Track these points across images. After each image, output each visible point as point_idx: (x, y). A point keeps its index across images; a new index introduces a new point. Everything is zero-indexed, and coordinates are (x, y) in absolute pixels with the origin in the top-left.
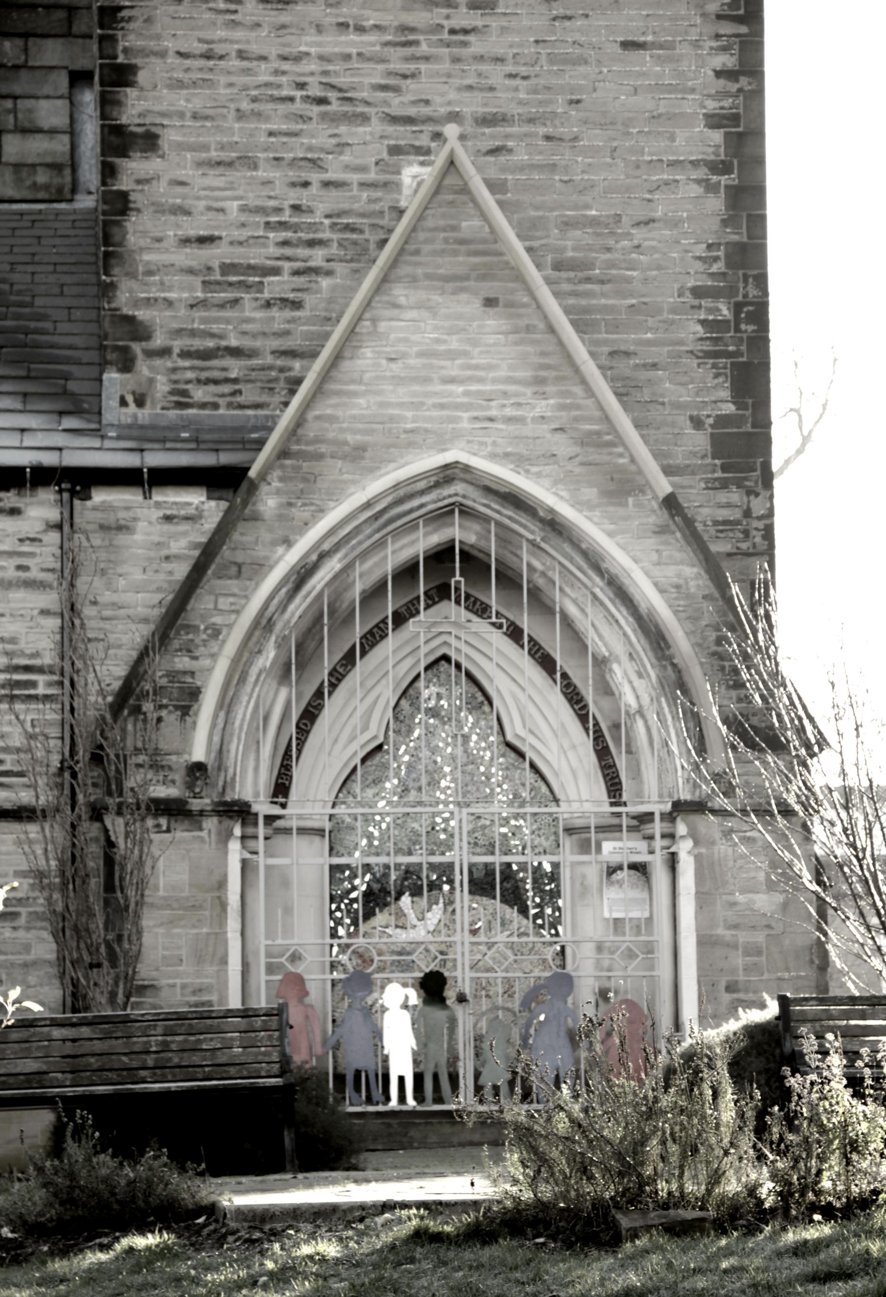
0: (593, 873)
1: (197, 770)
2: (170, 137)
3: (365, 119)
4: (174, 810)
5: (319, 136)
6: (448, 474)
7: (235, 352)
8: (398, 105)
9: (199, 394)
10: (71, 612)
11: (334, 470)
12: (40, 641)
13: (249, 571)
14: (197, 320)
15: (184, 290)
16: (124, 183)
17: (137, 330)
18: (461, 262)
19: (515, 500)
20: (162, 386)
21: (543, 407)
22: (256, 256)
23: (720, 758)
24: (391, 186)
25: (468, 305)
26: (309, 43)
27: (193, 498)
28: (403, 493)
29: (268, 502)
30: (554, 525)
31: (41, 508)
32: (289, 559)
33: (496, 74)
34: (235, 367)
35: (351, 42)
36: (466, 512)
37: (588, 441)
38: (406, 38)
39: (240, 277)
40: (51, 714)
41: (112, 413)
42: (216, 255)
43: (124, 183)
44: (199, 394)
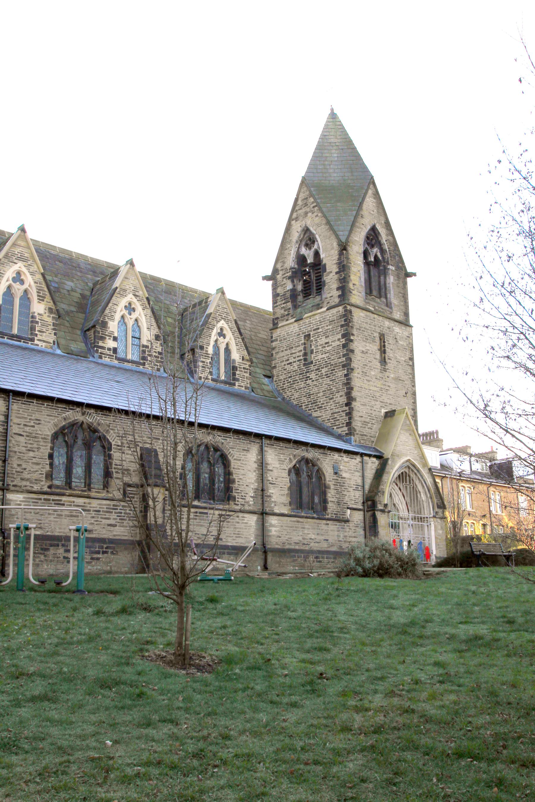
0: (407, 526)
1: (386, 505)
2: (358, 399)
3: (377, 401)
4: (383, 511)
5: (373, 403)
6: (409, 461)
7: (365, 435)
8: (381, 399)
9: (362, 441)
10: (363, 476)
11: (396, 458)
12: (360, 482)
13: (389, 473)
14: (361, 429)
15: (359, 424)
16: (353, 406)
17: (355, 430)
18: (407, 428)
19: (414, 466)
20: (358, 440)
21: (416, 452)
22: (367, 420)
23: (437, 509)
24: (381, 412)
25: (408, 434)
26: (371, 388)
27: (374, 460)
28: (403, 463)
29: (390, 462)
30: (418, 471)
31: (358, 458)
32: (394, 471)
33: (391, 397)
34: (365, 438)
35: (375, 389)
36: (409, 468)
37: (420, 458)
38: (381, 389)
39: (365, 423)
40: (361, 493)
41: (353, 443)
42: (363, 419)
43: (353, 406)
44: (362, 441)
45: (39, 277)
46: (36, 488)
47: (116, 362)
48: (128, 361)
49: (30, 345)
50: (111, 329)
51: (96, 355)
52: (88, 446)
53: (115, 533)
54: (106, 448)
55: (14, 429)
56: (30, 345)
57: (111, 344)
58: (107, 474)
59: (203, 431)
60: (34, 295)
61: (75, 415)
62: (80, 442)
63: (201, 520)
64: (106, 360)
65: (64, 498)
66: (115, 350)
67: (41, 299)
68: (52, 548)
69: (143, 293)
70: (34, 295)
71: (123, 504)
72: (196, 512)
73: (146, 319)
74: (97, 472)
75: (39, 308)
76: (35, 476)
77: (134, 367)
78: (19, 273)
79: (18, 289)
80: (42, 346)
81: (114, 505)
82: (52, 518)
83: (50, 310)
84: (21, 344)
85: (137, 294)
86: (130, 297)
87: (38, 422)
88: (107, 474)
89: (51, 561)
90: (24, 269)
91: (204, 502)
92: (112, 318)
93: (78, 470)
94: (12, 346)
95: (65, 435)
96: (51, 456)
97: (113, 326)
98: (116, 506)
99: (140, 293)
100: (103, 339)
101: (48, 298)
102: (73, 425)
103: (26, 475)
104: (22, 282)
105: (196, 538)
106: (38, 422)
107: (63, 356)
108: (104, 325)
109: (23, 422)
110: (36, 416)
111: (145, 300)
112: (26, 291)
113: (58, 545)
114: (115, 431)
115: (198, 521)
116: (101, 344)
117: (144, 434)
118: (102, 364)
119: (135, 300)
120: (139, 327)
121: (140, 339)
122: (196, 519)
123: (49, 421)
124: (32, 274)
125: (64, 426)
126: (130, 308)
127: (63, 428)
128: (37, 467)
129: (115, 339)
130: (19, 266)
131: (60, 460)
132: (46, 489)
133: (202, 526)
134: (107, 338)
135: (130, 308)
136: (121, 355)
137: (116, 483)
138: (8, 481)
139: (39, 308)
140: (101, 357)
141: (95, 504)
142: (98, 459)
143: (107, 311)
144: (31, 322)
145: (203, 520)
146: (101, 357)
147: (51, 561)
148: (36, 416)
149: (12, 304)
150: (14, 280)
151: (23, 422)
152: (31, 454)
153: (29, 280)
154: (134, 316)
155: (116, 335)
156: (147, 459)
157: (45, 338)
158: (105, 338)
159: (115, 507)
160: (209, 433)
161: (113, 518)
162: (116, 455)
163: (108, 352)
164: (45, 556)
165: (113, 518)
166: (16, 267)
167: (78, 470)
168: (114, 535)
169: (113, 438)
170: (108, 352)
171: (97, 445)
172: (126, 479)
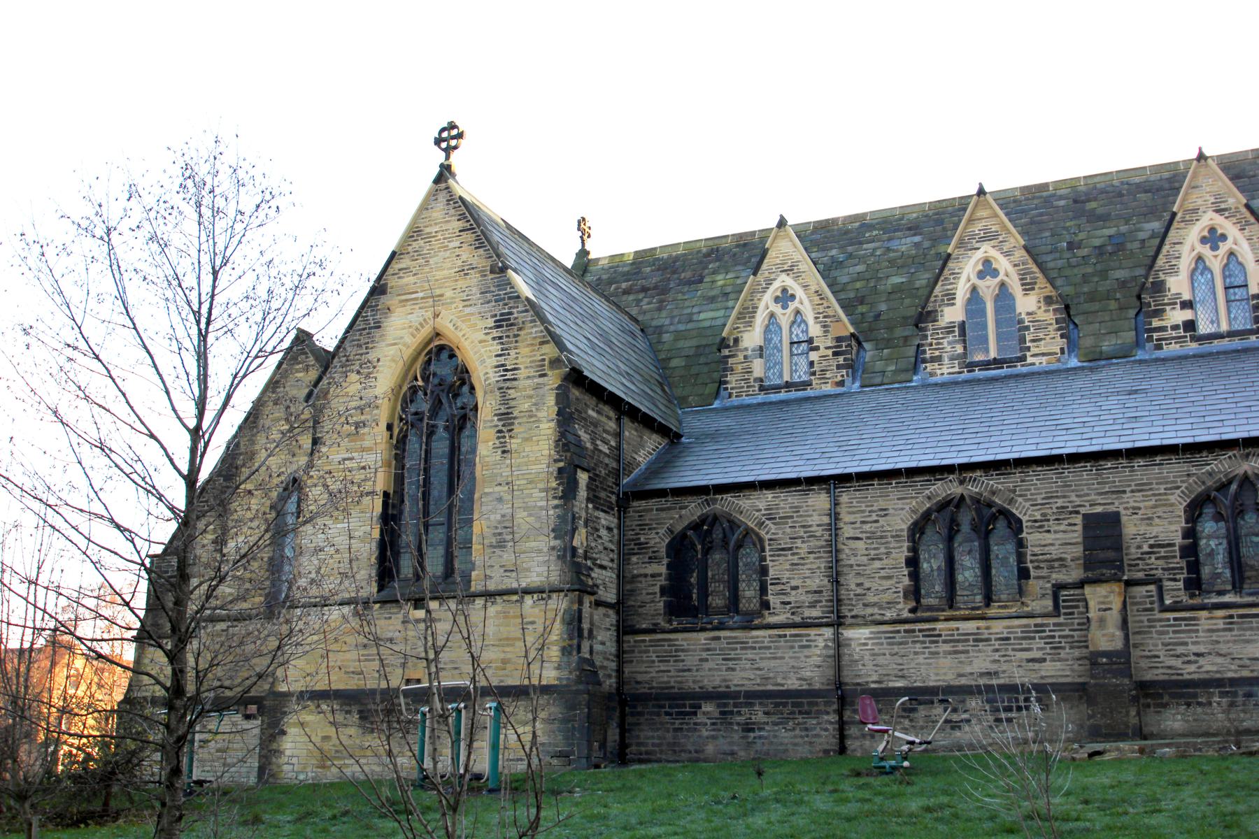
45: (1021, 254)
46: (889, 615)
47: (1194, 345)
48: (1219, 336)
49: (1019, 369)
50: (1173, 291)
51: (1149, 345)
52: (983, 532)
53: (1043, 673)
54: (1015, 526)
55: (847, 531)
56: (1019, 369)
57: (1178, 316)
58: (1024, 574)
59: (1230, 453)
60: (1016, 288)
61: (948, 488)
62: (965, 528)
63: (1244, 630)
64: (1172, 349)
65: (939, 626)
66: (1190, 325)
67: (1028, 287)
68: (921, 707)
69: (1236, 199)
70: (1016, 288)
71: (1052, 621)
72: (1231, 617)
73: (1251, 245)
74: (1003, 575)
75: (1027, 304)
76: (888, 596)
77: (1236, 343)
78: (987, 262)
79: (988, 287)
80: (1040, 363)
81: (1036, 625)
82: (921, 659)
83: (1048, 300)
84: (1005, 371)
85: (1223, 206)
86: (1209, 218)
87: (884, 512)
88: (1024, 574)
89: (922, 728)
90: (994, 253)
91: (1251, 594)
92: (1173, 270)
93: (968, 572)
94: (978, 381)
95: (939, 522)
96: (913, 562)
97: (1178, 285)
98: (1042, 625)
99: (1231, 202)
100: (1158, 313)
101: (1041, 281)
102: (944, 505)
103: (871, 598)
104: (995, 273)
105: (1233, 667)
106: (884, 512)
107: (1082, 368)
108: (1159, 287)
109: (858, 517)
110: (882, 503)
111: (1244, 210)
112: (1003, 285)
113: (932, 703)
114: (1028, 499)
115: (1235, 633)
116: (1156, 323)
117: (1089, 492)
118: (1164, 360)
119: (1219, 220)
120: (1240, 264)
121: (1246, 286)
122: (1230, 630)
123: (901, 508)
124: (1007, 254)
125: (929, 509)
126: (1213, 238)
127: (926, 516)
128: (887, 583)
129: (1188, 305)
130: (986, 250)
131: (932, 563)
132: (906, 614)
133: (1248, 641)
134: (1168, 308)
135: (1213, 238)
136: (1204, 328)
137: (1034, 585)
138: (845, 611)
139: (1027, 304)
140: (1159, 347)
141: (998, 627)
142: (1002, 550)
143: (1161, 261)
144: (1015, 329)
145: (1251, 629)
146: (1159, 347)
147: (922, 728)
148: (882, 503)
149: (983, 312)
150: (981, 275)
151: (858, 517)
152: (877, 564)
153: (1003, 264)
154: (1224, 248)
155: (1186, 296)
156: (1103, 534)
157: (1046, 347)
158: (1164, 311)
159: (1039, 628)
160: (1247, 455)
161: (1037, 647)
162: (1032, 538)
163: (1174, 334)
164: (911, 721)
165: (1037, 647)
166: (979, 255)
167: (968, 572)
168: (1042, 678)
169: (1024, 511)
170: (1174, 334)
171: (1001, 524)
172: (1059, 577)
